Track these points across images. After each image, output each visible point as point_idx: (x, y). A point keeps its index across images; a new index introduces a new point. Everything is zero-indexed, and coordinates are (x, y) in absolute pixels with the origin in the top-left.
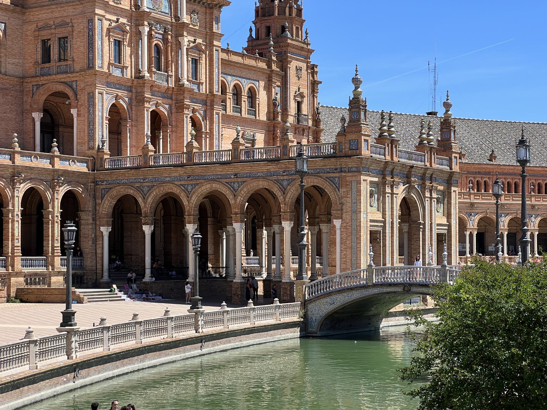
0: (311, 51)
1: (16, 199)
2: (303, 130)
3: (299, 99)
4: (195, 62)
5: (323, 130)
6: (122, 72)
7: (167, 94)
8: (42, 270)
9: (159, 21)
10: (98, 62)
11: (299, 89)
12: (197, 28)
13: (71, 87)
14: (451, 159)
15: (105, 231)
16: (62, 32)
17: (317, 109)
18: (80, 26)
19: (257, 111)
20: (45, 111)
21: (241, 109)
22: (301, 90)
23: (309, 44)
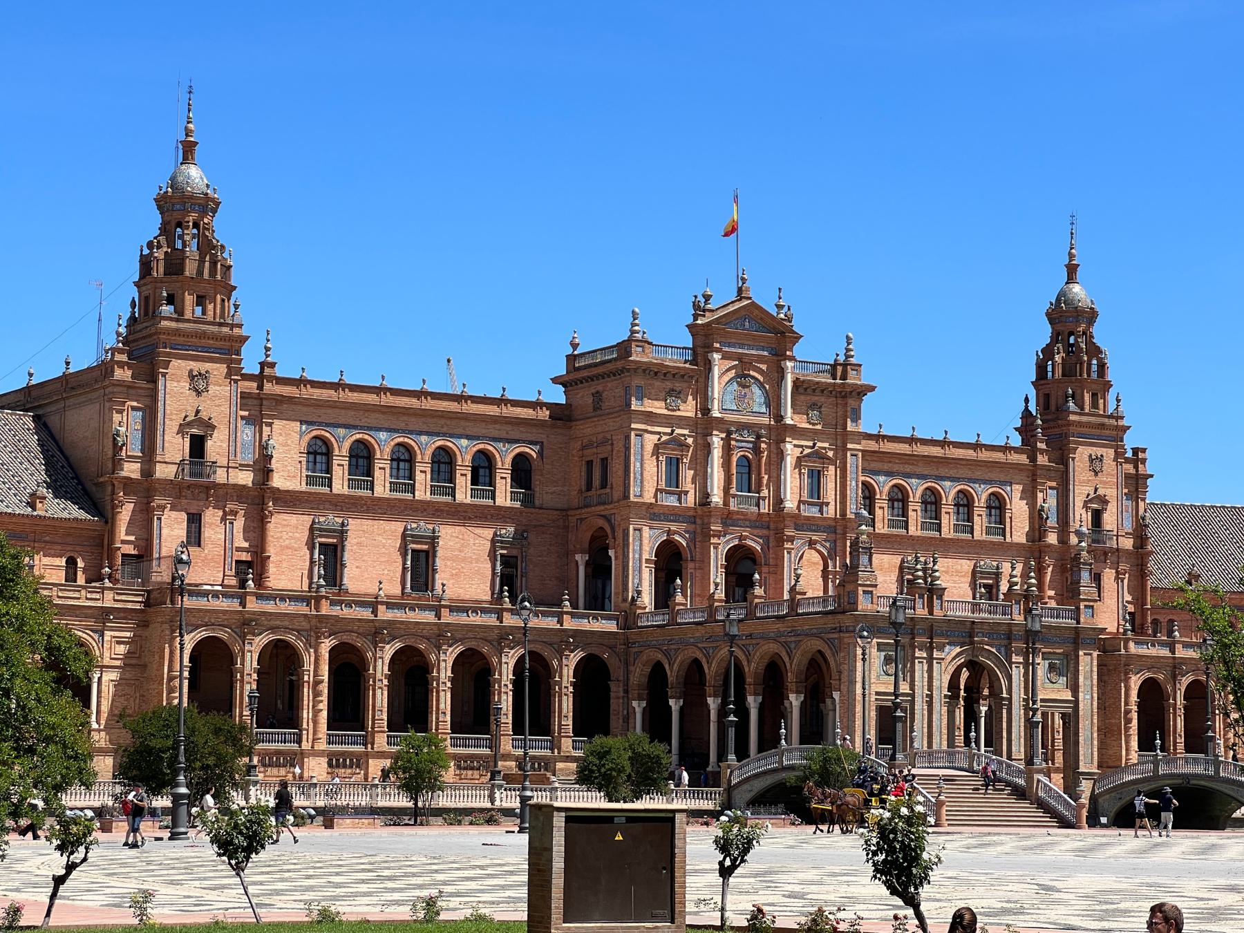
0: (1126, 429)
1: (504, 666)
2: (1105, 554)
4: (816, 478)
5: (1152, 552)
6: (680, 500)
7: (759, 523)
8: (548, 753)
9: (742, 427)
10: (634, 490)
11: (1096, 490)
12: (819, 427)
13: (609, 521)
14: (1078, 609)
15: (638, 706)
16: (603, 451)
17: (1143, 519)
18: (619, 446)
19: (1008, 529)
20: (590, 551)
21: (972, 527)
22: (1100, 492)
23: (1122, 418)
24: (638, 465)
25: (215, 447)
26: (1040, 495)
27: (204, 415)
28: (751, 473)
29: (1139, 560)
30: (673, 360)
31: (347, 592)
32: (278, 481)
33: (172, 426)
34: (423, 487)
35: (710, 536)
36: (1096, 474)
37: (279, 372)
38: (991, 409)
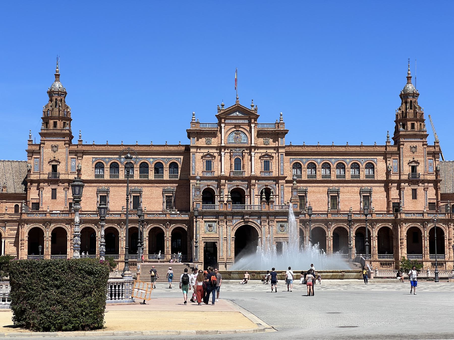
3: (413, 164)
22: (416, 159)
24: (193, 164)
25: (60, 168)
26: (388, 162)
27: (56, 159)
28: (238, 164)
29: (436, 183)
30: (208, 128)
31: (109, 211)
32: (83, 177)
33: (46, 163)
34: (137, 175)
35: (221, 186)
36: (413, 153)
37: (84, 143)
38: (380, 132)
